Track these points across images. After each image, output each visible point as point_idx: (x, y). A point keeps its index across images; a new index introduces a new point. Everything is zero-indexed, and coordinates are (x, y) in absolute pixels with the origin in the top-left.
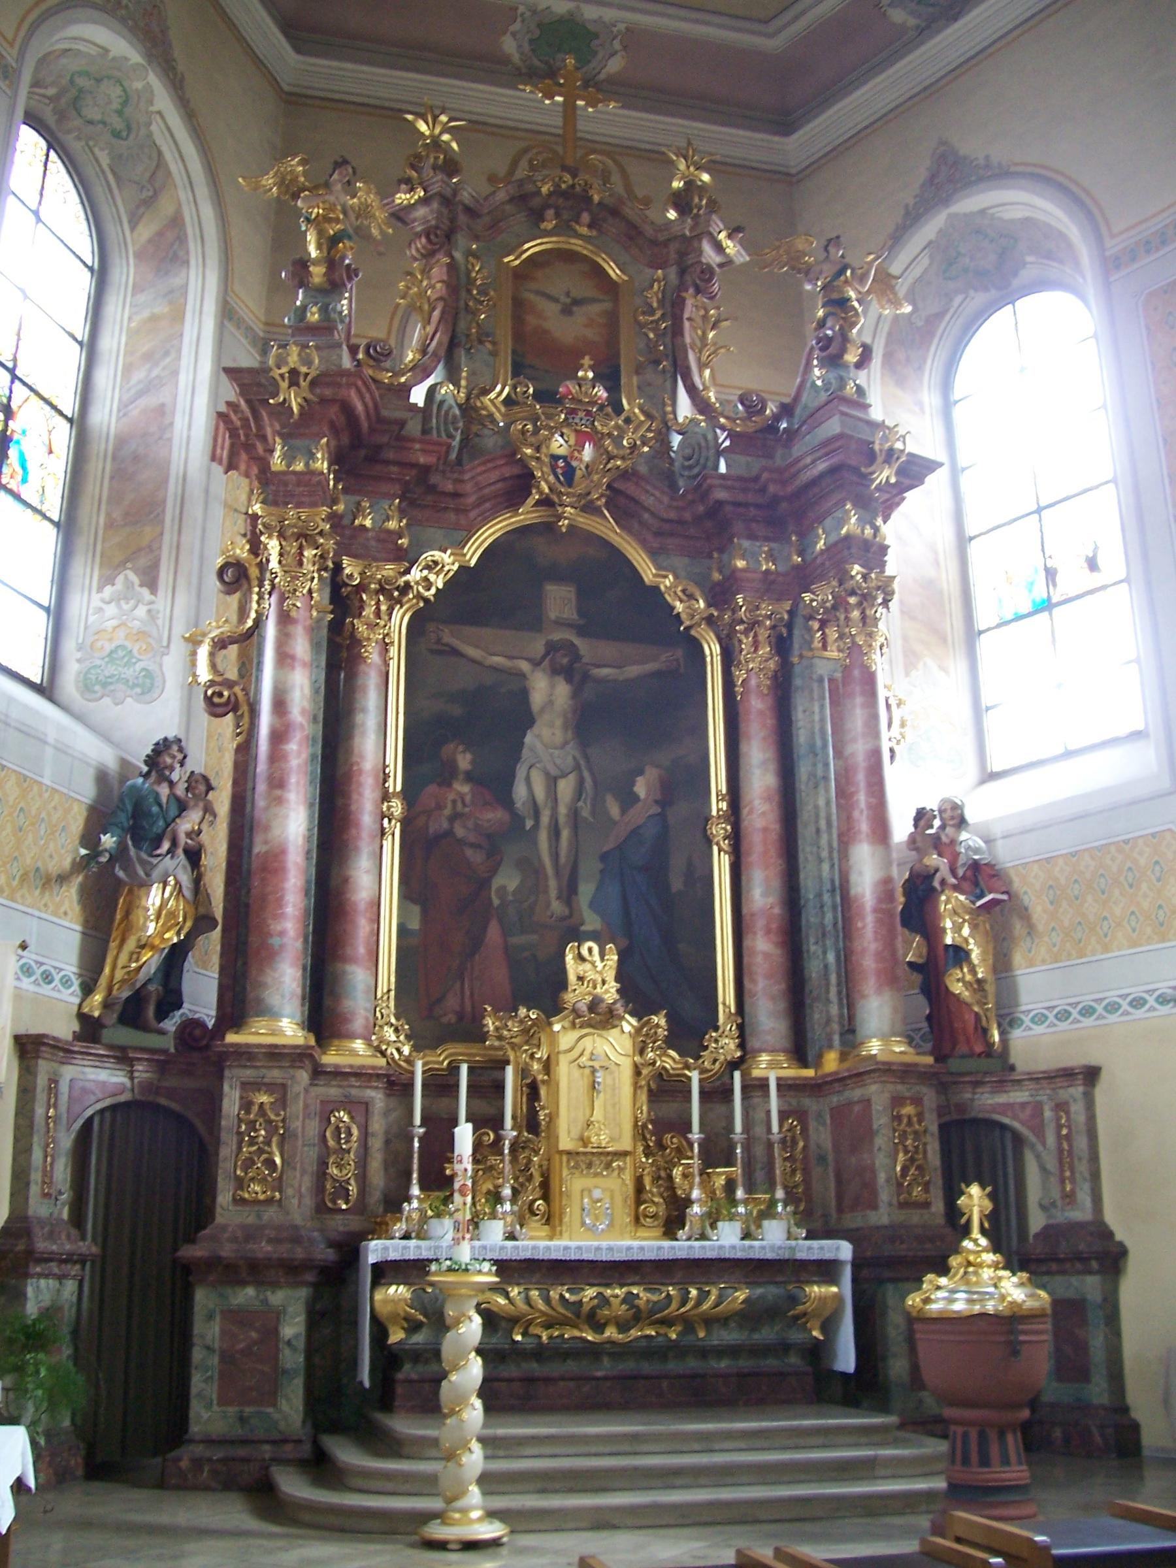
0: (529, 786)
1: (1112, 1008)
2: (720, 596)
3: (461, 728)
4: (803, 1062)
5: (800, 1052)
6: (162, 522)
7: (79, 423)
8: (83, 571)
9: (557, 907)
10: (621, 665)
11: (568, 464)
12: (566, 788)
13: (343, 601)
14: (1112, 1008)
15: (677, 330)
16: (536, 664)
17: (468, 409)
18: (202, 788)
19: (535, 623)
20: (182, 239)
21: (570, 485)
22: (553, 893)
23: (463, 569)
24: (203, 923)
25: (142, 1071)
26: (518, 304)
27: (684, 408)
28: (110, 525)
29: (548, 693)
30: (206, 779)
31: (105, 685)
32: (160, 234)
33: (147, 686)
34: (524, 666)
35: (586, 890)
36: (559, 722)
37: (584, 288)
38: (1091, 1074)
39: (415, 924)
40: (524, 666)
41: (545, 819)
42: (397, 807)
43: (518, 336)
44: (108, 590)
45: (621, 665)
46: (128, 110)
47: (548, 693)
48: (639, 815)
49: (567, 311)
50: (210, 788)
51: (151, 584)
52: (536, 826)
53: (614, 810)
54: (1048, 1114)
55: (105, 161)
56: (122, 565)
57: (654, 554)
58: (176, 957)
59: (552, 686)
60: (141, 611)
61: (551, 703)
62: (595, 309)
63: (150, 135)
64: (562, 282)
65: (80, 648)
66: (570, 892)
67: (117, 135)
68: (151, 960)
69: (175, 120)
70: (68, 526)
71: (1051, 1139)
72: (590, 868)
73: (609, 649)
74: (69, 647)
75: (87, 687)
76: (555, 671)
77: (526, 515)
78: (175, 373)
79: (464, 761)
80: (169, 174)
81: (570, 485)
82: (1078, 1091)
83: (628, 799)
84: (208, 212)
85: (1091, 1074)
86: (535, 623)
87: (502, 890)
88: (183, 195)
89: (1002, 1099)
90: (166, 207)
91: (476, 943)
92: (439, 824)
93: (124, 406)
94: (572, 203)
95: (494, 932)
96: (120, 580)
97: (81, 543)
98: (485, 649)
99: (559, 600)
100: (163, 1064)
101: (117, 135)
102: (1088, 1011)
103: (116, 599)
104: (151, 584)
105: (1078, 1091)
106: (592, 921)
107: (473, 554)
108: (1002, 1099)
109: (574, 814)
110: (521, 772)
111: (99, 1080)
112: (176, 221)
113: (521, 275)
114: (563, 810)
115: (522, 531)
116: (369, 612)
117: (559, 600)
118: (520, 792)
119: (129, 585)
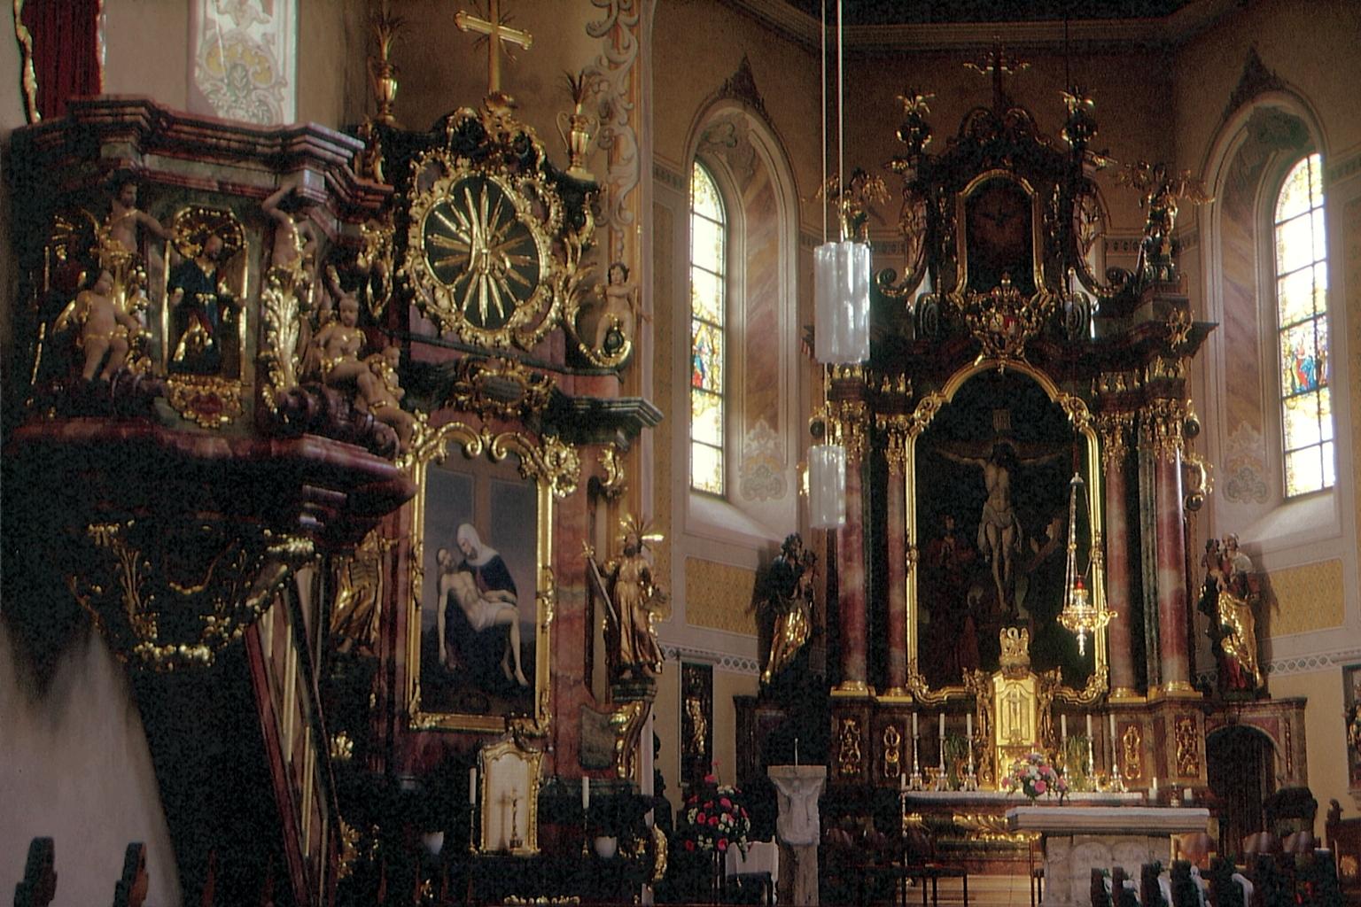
0: (986, 535)
1: (1313, 663)
3: (948, 498)
4: (1144, 693)
5: (1140, 687)
6: (777, 388)
7: (727, 330)
8: (739, 422)
9: (1003, 606)
11: (1001, 338)
12: (1007, 535)
13: (878, 440)
14: (1313, 663)
16: (988, 460)
17: (943, 303)
18: (811, 559)
20: (771, 197)
21: (1003, 348)
22: (1002, 598)
23: (945, 405)
28: (749, 392)
29: (996, 477)
30: (813, 555)
31: (755, 490)
32: (759, 195)
34: (981, 462)
35: (1020, 597)
36: (1002, 496)
38: (1301, 703)
39: (927, 621)
40: (981, 462)
41: (996, 555)
42: (914, 554)
44: (752, 432)
46: (736, 133)
47: (996, 477)
49: (1000, 225)
50: (815, 559)
51: (775, 426)
52: (991, 560)
53: (1035, 548)
54: (1281, 725)
55: (724, 158)
56: (758, 417)
59: (998, 473)
60: (771, 444)
61: (997, 484)
63: (748, 142)
65: (740, 469)
67: (729, 146)
69: (763, 133)
70: (727, 397)
71: (1282, 740)
72: (1022, 584)
74: (735, 467)
76: (1000, 465)
78: (777, 288)
80: (760, 159)
81: (1003, 348)
82: (1293, 711)
84: (786, 180)
85: (1301, 703)
87: (974, 600)
88: (770, 170)
89: (1255, 715)
90: (761, 179)
93: (750, 313)
96: (758, 425)
97: (735, 404)
99: (1001, 421)
101: (729, 146)
102: (1303, 664)
103: (757, 437)
104: (775, 426)
105: (1293, 711)
106: (1023, 614)
107: (949, 393)
108: (1255, 715)
109: (1012, 549)
110: (981, 529)
112: (768, 187)
113: (971, 203)
114: (1005, 549)
116: (892, 444)
117: (1001, 421)
118: (982, 540)
119: (763, 428)
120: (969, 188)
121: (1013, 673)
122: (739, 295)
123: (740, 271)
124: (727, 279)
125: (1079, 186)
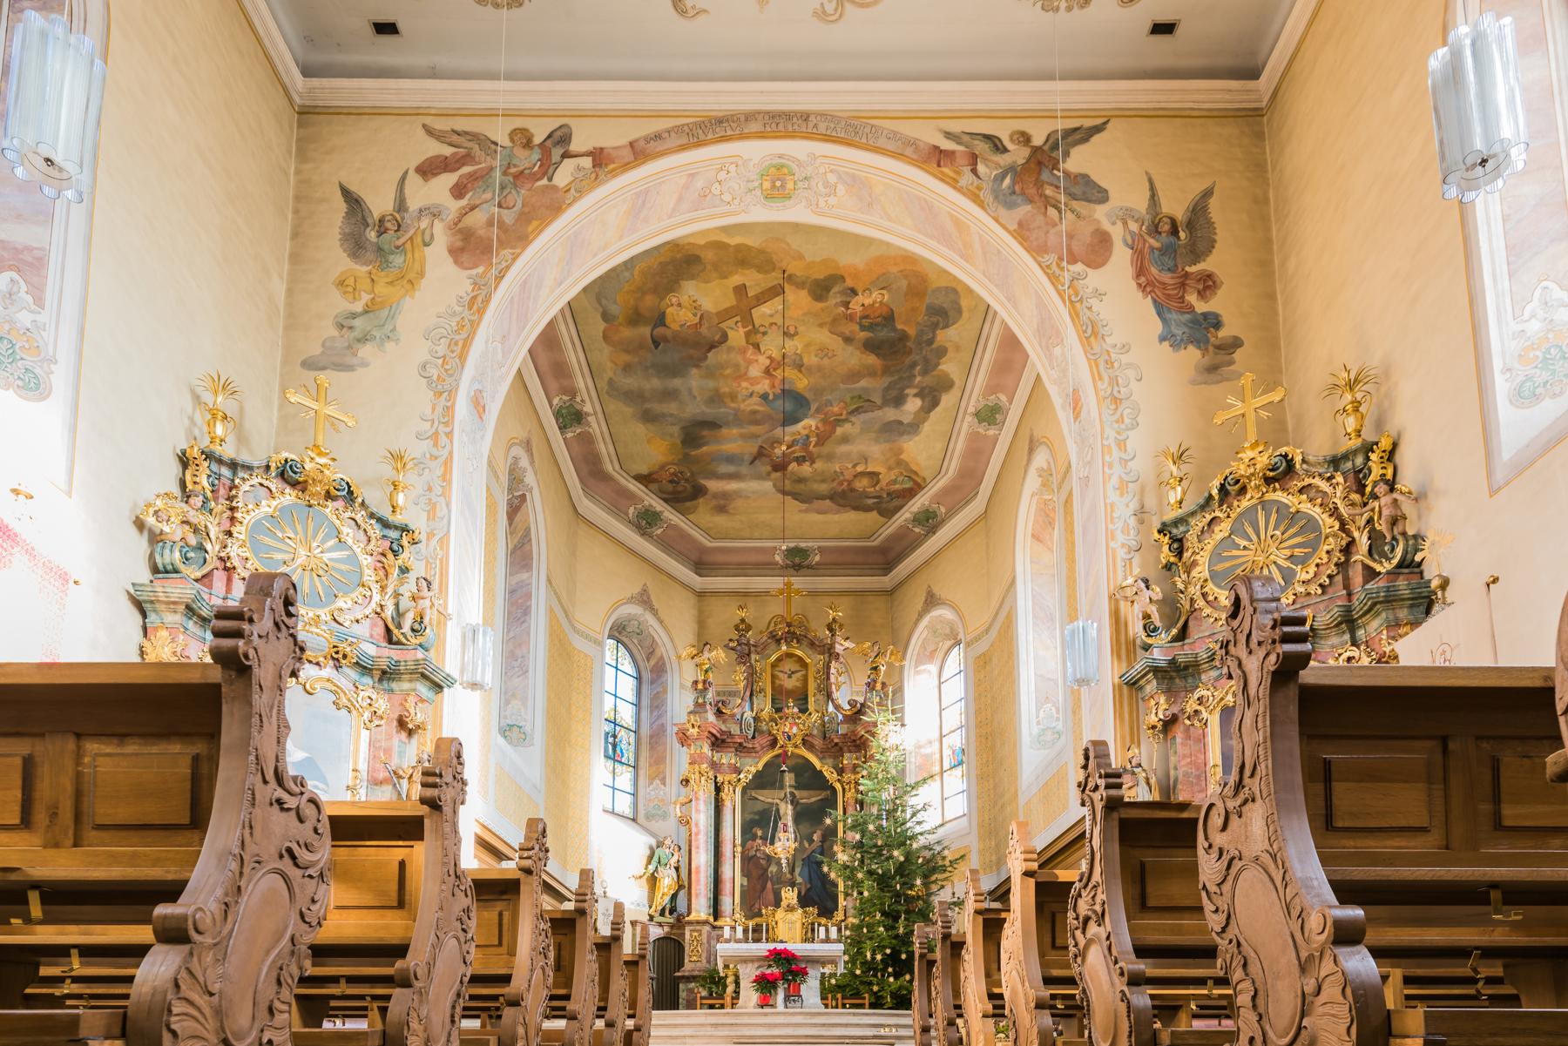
2: (840, 772)
10: (809, 798)
15: (828, 678)
19: (782, 787)
24: (681, 887)
25: (666, 929)
26: (773, 676)
27: (831, 708)
29: (787, 811)
33: (664, 816)
35: (798, 870)
37: (795, 667)
43: (773, 688)
45: (809, 798)
48: (814, 846)
57: (821, 759)
58: (674, 897)
62: (799, 675)
64: (789, 665)
66: (792, 871)
68: (667, 899)
73: (805, 793)
75: (648, 817)
77: (777, 751)
79: (759, 833)
83: (811, 841)
86: (782, 787)
91: (764, 888)
92: (752, 853)
94: (791, 637)
95: (769, 884)
97: (642, 772)
98: (766, 797)
100: (672, 926)
107: (760, 766)
111: (656, 932)
113: (774, 666)
115: (777, 756)
117: (789, 779)
120: (773, 658)
121: (790, 909)
122: (645, 714)
123: (645, 702)
124: (638, 705)
125: (830, 652)
